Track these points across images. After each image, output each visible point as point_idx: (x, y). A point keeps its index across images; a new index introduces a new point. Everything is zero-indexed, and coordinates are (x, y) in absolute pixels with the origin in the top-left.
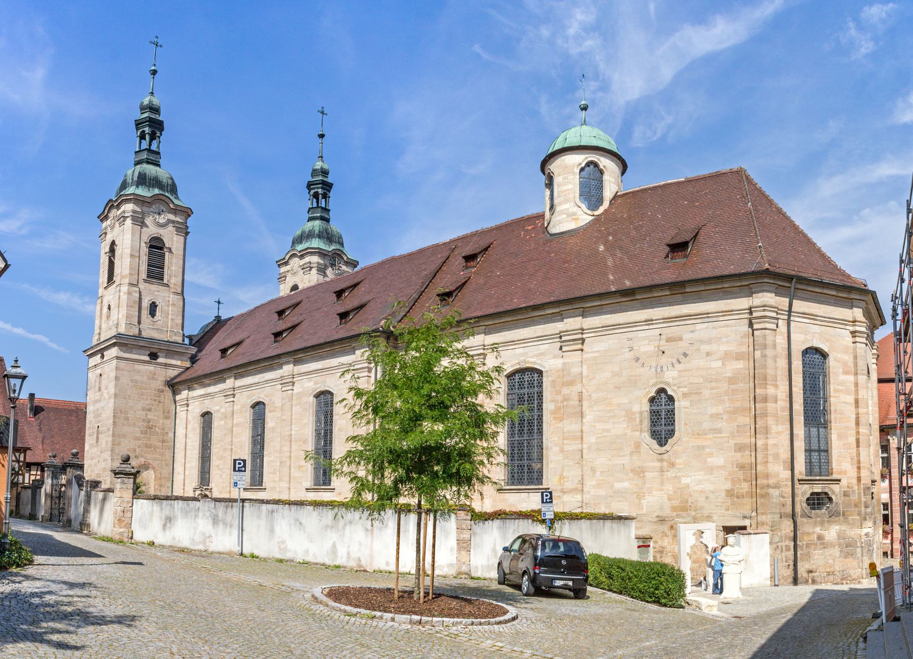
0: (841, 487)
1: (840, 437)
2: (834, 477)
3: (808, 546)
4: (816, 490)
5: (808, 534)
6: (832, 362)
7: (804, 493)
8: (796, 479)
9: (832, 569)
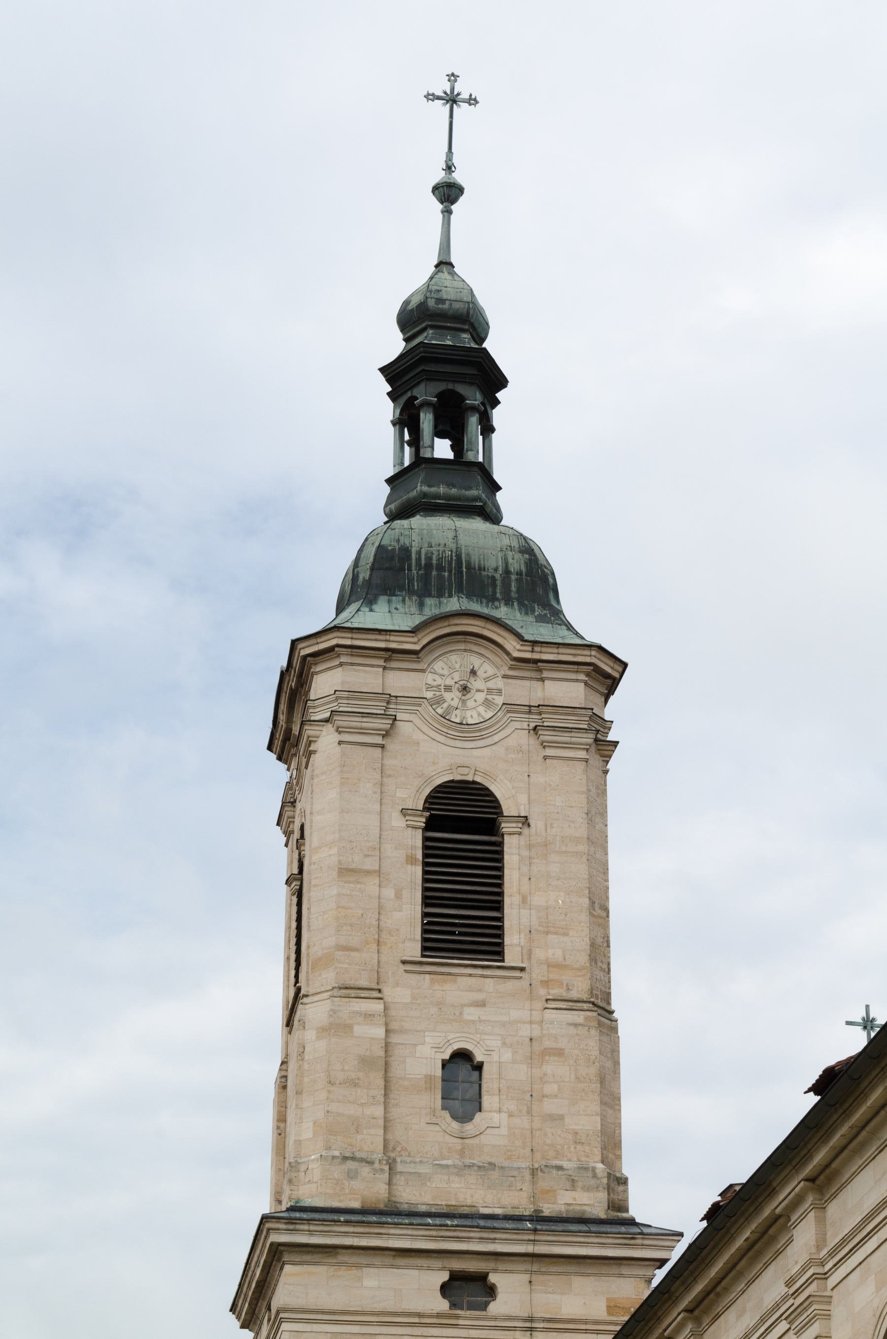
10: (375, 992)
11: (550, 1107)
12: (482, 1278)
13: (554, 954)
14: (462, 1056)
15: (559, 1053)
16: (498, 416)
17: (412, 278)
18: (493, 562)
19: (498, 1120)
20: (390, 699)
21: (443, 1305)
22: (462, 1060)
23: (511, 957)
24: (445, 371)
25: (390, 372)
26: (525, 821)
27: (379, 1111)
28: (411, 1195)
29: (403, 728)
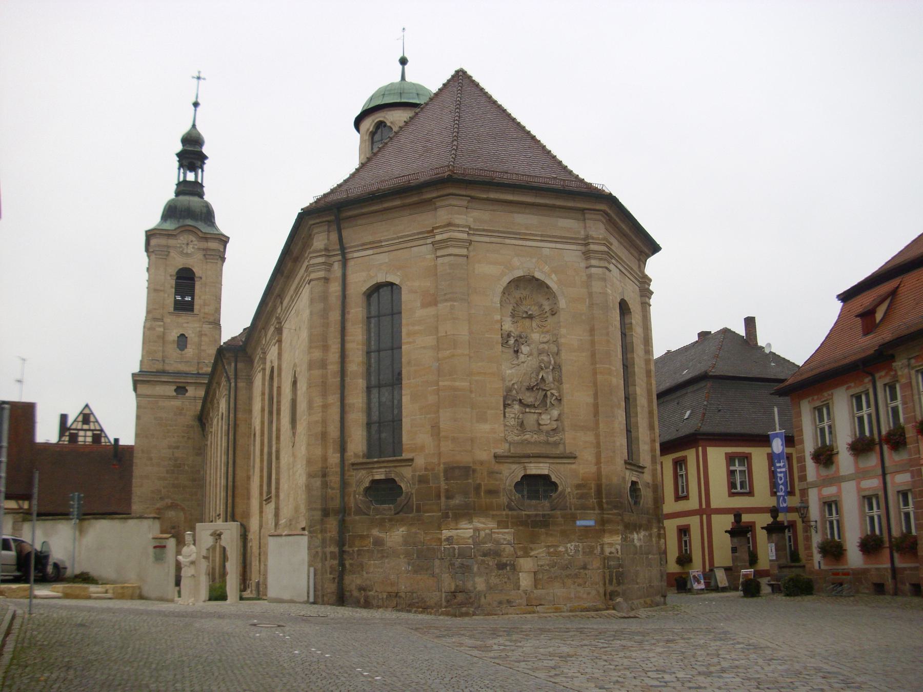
0: (414, 471)
2: (405, 456)
3: (359, 552)
4: (377, 477)
5: (362, 537)
6: (405, 296)
7: (360, 482)
8: (347, 463)
9: (395, 589)
10: (162, 320)
11: (203, 348)
12: (184, 388)
13: (206, 311)
14: (183, 335)
15: (206, 335)
16: (205, 167)
17: (185, 128)
19: (190, 351)
20: (168, 247)
21: (175, 394)
22: (183, 337)
23: (196, 311)
24: (192, 154)
25: (178, 155)
26: (201, 278)
27: (161, 349)
28: (168, 368)
29: (172, 254)
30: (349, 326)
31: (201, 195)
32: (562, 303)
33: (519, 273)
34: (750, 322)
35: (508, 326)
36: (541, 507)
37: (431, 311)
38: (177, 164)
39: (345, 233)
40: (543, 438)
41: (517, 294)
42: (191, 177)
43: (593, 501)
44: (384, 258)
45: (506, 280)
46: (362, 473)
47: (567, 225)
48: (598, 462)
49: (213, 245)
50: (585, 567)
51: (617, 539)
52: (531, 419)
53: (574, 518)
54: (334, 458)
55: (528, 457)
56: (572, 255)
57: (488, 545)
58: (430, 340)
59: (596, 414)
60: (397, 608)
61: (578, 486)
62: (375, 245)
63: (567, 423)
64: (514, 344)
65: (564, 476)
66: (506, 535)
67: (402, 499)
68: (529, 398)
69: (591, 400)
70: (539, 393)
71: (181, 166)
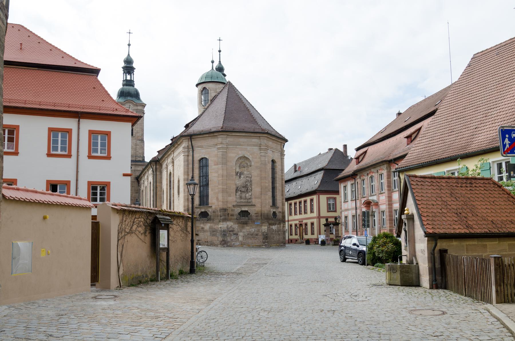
1: (212, 190)
2: (210, 205)
6: (210, 162)
17: (125, 56)
18: (133, 93)
25: (123, 68)
30: (194, 169)
31: (133, 86)
32: (253, 164)
33: (241, 156)
34: (345, 146)
35: (238, 170)
36: (244, 219)
37: (216, 167)
38: (122, 72)
39: (193, 142)
40: (246, 201)
41: (241, 161)
42: (128, 78)
43: (260, 218)
44: (204, 151)
45: (237, 158)
46: (198, 210)
47: (255, 141)
48: (261, 207)
49: (140, 108)
50: (257, 235)
51: (266, 227)
52: (243, 195)
53: (254, 222)
54: (190, 206)
55: (242, 206)
56: (256, 149)
57: (231, 229)
58: (216, 175)
59: (261, 194)
60: (207, 245)
61: (256, 214)
62: (201, 147)
63: (253, 196)
64: (239, 174)
65: (252, 210)
66: (236, 227)
67: (209, 217)
68: (243, 189)
69: (260, 190)
70: (246, 188)
71: (124, 72)
